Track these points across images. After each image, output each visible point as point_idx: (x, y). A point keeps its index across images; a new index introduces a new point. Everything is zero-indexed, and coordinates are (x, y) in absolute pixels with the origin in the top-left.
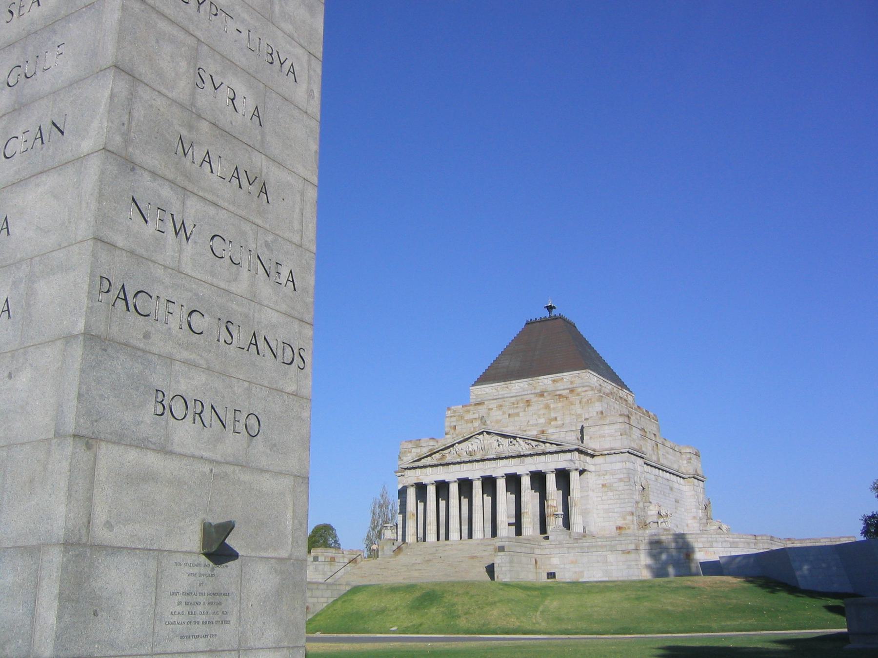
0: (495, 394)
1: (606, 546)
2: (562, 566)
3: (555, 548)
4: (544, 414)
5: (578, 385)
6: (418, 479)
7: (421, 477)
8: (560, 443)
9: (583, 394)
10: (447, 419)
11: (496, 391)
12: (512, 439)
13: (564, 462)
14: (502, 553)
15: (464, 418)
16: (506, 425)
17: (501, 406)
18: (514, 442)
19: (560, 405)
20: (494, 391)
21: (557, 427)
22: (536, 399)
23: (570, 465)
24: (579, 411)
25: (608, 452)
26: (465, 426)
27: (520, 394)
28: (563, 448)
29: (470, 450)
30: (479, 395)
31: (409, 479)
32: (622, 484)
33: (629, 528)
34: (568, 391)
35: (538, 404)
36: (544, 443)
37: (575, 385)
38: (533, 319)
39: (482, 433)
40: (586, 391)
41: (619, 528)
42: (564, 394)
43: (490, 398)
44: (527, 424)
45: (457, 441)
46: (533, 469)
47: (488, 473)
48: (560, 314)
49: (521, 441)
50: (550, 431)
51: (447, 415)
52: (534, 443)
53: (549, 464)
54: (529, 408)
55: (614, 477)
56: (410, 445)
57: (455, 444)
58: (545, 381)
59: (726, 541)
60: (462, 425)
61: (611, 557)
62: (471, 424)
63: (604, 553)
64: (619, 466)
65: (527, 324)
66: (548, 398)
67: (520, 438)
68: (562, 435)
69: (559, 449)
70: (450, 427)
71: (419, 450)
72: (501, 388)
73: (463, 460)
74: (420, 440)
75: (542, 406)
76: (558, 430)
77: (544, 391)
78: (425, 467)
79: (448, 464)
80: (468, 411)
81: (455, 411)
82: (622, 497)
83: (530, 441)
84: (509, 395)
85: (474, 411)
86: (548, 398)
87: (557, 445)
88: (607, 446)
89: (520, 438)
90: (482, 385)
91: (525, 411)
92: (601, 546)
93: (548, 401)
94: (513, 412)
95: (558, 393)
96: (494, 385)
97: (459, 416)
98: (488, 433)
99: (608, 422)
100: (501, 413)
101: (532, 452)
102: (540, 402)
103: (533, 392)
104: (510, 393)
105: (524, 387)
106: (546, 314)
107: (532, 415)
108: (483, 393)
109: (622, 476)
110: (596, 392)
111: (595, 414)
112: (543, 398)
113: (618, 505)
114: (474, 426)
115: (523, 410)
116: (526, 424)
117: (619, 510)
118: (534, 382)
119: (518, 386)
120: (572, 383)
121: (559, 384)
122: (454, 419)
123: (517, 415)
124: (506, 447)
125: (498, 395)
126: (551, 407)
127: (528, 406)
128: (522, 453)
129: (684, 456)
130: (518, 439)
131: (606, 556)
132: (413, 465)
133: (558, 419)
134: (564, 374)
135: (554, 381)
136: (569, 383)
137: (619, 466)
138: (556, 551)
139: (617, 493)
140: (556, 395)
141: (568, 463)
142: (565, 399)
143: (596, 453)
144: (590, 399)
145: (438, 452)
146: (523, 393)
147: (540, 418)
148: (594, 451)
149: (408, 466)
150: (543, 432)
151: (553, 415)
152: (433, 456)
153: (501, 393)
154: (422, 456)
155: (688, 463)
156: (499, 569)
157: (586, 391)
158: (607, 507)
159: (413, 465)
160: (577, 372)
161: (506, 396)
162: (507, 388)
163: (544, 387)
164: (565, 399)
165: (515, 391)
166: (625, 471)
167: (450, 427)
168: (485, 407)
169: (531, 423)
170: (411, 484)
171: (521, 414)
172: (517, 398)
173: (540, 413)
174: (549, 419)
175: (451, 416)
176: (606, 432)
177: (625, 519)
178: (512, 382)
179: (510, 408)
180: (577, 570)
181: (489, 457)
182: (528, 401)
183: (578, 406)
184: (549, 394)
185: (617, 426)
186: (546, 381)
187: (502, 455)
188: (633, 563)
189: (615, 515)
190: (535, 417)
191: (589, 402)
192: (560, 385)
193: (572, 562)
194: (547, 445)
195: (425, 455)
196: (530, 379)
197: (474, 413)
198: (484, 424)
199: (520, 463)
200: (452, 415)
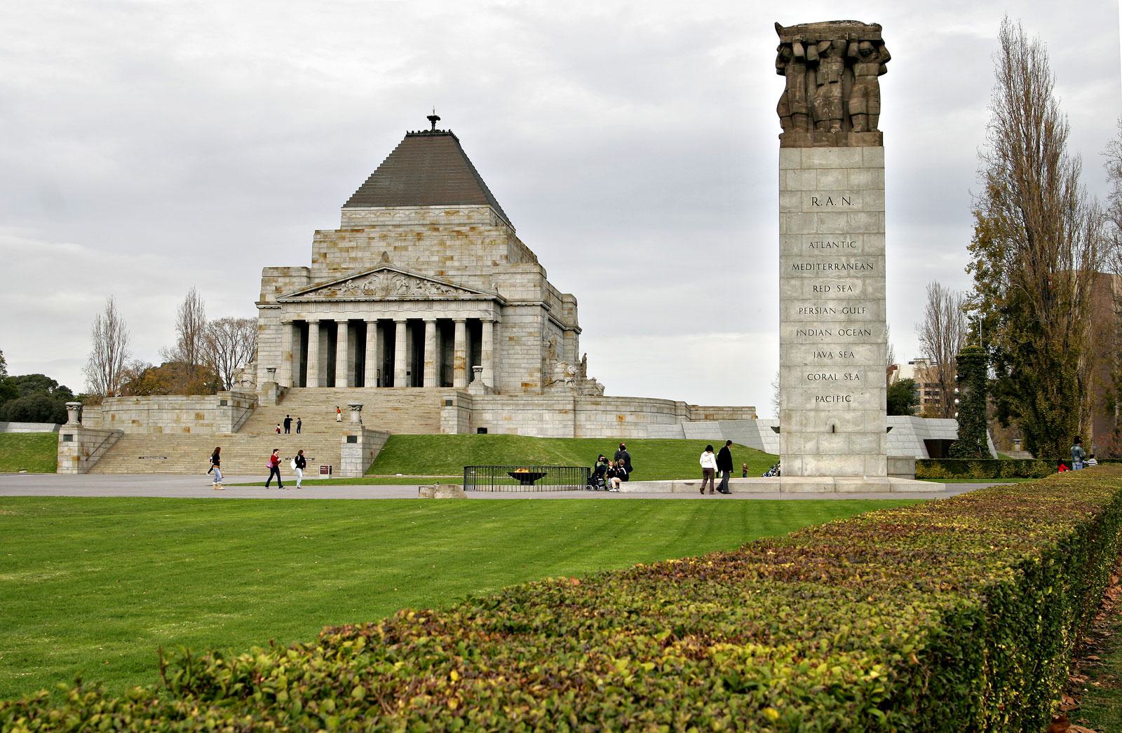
1: (542, 405)
2: (495, 422)
3: (488, 404)
4: (438, 251)
6: (299, 316)
7: (303, 314)
9: (486, 233)
10: (316, 244)
12: (418, 282)
14: (450, 407)
17: (385, 236)
19: (458, 243)
21: (458, 270)
22: (429, 233)
24: (480, 253)
25: (519, 303)
26: (338, 255)
27: (403, 223)
31: (287, 315)
32: (532, 338)
33: (536, 385)
34: (468, 228)
35: (431, 240)
37: (472, 221)
38: (416, 131)
39: (382, 271)
40: (489, 231)
41: (525, 385)
43: (367, 223)
46: (442, 316)
47: (387, 316)
49: (429, 284)
50: (451, 273)
52: (444, 288)
53: (459, 314)
55: (524, 330)
56: (276, 274)
58: (437, 212)
59: (654, 406)
60: (334, 253)
61: (547, 416)
62: (346, 254)
63: (540, 412)
64: (530, 319)
65: (409, 136)
68: (465, 279)
70: (319, 254)
71: (287, 280)
74: (289, 268)
75: (436, 242)
76: (459, 273)
78: (308, 302)
79: (337, 302)
80: (344, 238)
81: (325, 236)
82: (530, 352)
84: (390, 223)
86: (444, 234)
87: (472, 292)
88: (518, 297)
89: (428, 281)
92: (538, 405)
95: (457, 229)
96: (372, 208)
97: (331, 242)
98: (389, 271)
103: (421, 222)
106: (428, 126)
108: (358, 216)
109: (532, 330)
110: (502, 233)
111: (498, 258)
113: (525, 361)
117: (527, 366)
118: (423, 211)
119: (402, 214)
120: (469, 217)
121: (453, 218)
122: (324, 245)
123: (406, 248)
124: (415, 291)
127: (419, 239)
129: (565, 306)
131: (541, 415)
133: (455, 258)
134: (461, 206)
135: (447, 213)
137: (530, 319)
138: (490, 407)
139: (526, 347)
143: (508, 304)
145: (326, 287)
146: (409, 223)
147: (432, 255)
148: (505, 300)
150: (442, 273)
151: (449, 253)
153: (379, 219)
155: (569, 313)
156: (446, 423)
157: (489, 231)
158: (513, 361)
160: (477, 206)
161: (387, 223)
166: (535, 325)
167: (319, 254)
168: (364, 235)
169: (421, 259)
172: (407, 229)
176: (518, 281)
177: (531, 376)
180: (511, 426)
184: (445, 229)
185: (531, 277)
186: (437, 212)
188: (570, 423)
189: (522, 370)
191: (493, 243)
192: (455, 219)
193: (506, 419)
194: (461, 291)
196: (418, 207)
197: (350, 241)
198: (386, 261)
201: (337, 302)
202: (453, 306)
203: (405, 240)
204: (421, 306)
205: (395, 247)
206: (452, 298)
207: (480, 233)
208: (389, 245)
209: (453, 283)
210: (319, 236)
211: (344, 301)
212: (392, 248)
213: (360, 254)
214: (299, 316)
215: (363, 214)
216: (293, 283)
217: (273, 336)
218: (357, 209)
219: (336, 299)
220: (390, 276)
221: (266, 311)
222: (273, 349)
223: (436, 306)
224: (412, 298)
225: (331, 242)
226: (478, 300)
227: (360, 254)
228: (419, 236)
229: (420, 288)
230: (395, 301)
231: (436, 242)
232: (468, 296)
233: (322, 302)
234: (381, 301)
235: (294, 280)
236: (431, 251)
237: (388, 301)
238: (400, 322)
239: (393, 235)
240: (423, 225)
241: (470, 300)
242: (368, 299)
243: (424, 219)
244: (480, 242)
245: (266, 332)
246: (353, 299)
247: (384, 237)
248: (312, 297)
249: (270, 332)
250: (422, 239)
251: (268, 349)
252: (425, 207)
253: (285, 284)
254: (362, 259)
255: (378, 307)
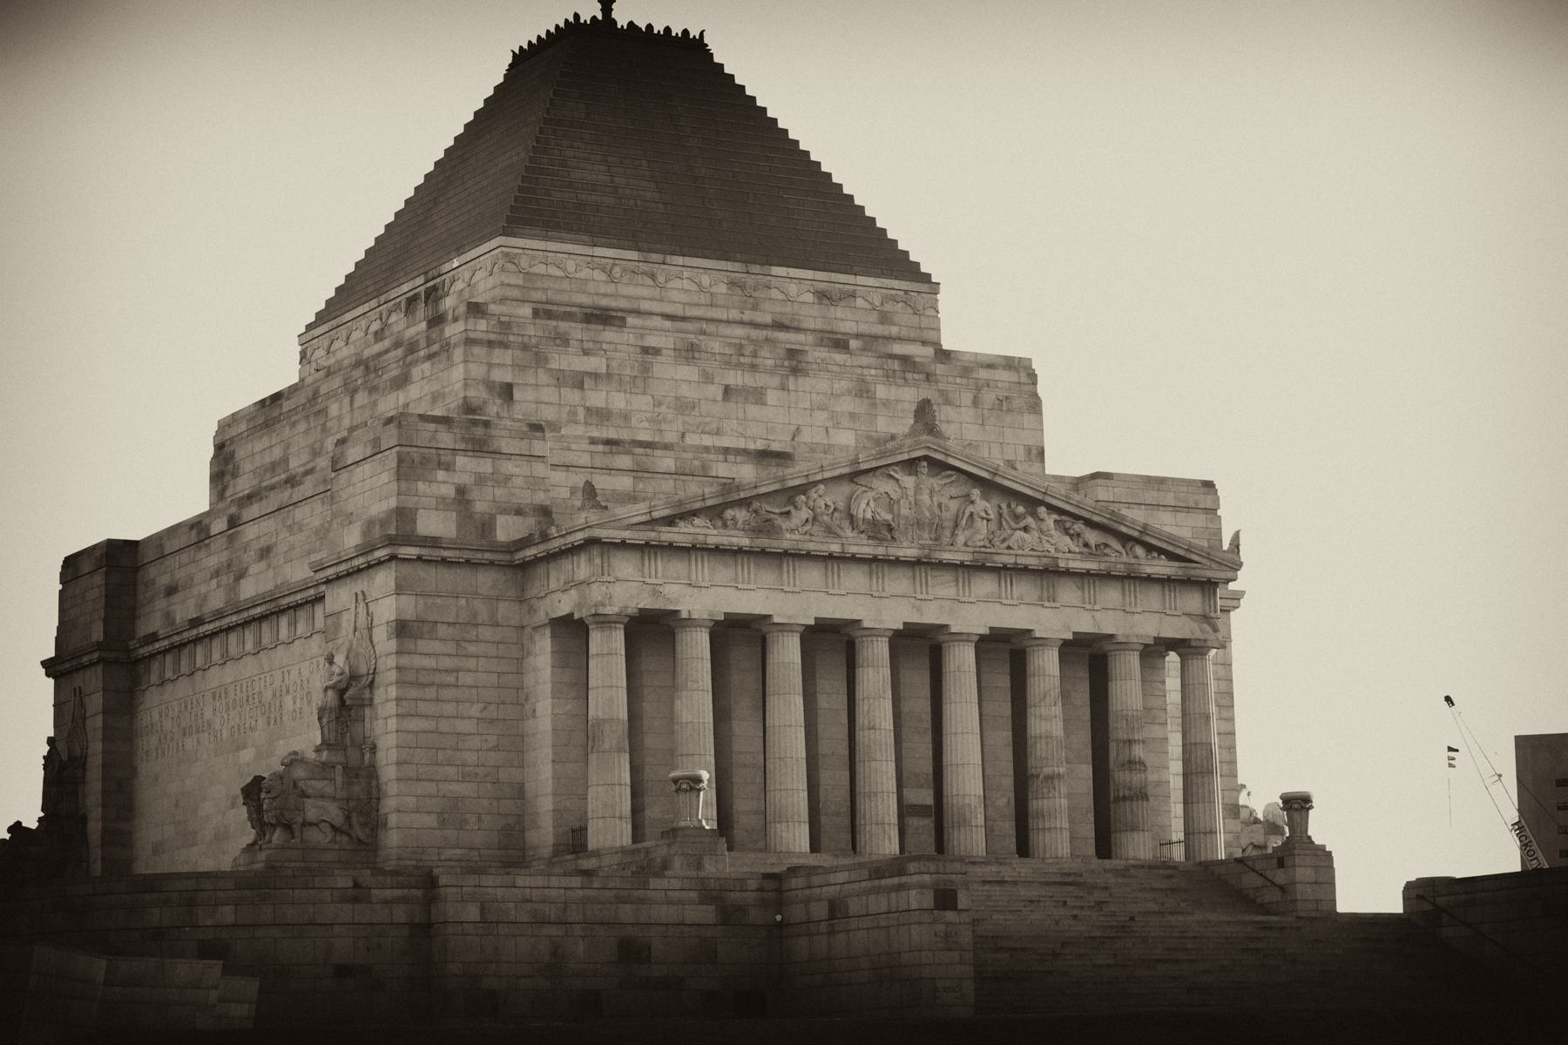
0: (602, 290)
4: (852, 416)
5: (904, 333)
6: (656, 593)
8: (1181, 553)
9: (983, 374)
10: (477, 350)
11: (603, 277)
12: (1021, 509)
13: (1187, 618)
15: (546, 360)
16: (714, 426)
18: (1030, 520)
20: (599, 275)
23: (1202, 631)
26: (549, 394)
28: (1192, 572)
29: (869, 516)
30: (537, 275)
36: (1125, 539)
37: (894, 330)
42: (917, 359)
44: (793, 439)
45: (827, 475)
46: (1085, 624)
48: (702, 33)
49: (1050, 520)
51: (472, 335)
52: (1093, 537)
54: (801, 380)
56: (446, 439)
57: (815, 484)
66: (865, 360)
67: (1052, 508)
69: (1180, 573)
70: (490, 385)
71: (485, 466)
72: (624, 270)
73: (853, 549)
77: (787, 322)
80: (563, 340)
81: (506, 326)
83: (1078, 527)
85: (586, 345)
89: (1052, 508)
90: (547, 239)
91: (783, 388)
93: (866, 372)
94: (740, 383)
95: (898, 349)
96: (598, 251)
98: (938, 466)
99: (1169, 499)
100: (696, 378)
101: (1091, 565)
102: (835, 368)
103: (748, 316)
104: (661, 300)
105: (713, 290)
107: (812, 409)
111: (1021, 452)
112: (844, 357)
114: (587, 405)
115: (776, 381)
116: (789, 438)
118: (750, 280)
120: (885, 318)
121: (839, 312)
122: (499, 356)
123: (758, 396)
125: (615, 296)
126: (878, 396)
127: (795, 371)
128: (1062, 564)
130: (1042, 510)
132: (653, 535)
134: (861, 280)
135: (823, 296)
136: (875, 315)
140: (892, 357)
141: (1195, 625)
142: (922, 376)
144: (1007, 398)
147: (837, 425)
149: (627, 534)
152: (729, 513)
154: (689, 507)
159: (653, 535)
161: (645, 306)
162: (653, 277)
163: (788, 309)
164: (922, 376)
165: (684, 298)
167: (490, 385)
168: (627, 337)
170: (630, 611)
171: (772, 396)
173: (837, 408)
174: (869, 438)
175: (490, 344)
178: (669, 259)
179: (728, 364)
181: (947, 556)
182: (792, 353)
183: (967, 414)
185: (1200, 520)
186: (793, 288)
187: (996, 558)
190: (821, 417)
191: (1003, 404)
194: (1139, 551)
195: (698, 505)
196: (737, 266)
197: (586, 353)
199: (1040, 598)
200: (492, 337)
201: (786, 555)
202: (1112, 595)
203: (754, 367)
204: (1024, 589)
205: (727, 390)
206: (1120, 569)
207: (966, 371)
208: (707, 378)
209: (1121, 520)
210: (482, 325)
211: (809, 556)
212: (715, 391)
213: (618, 401)
214: (656, 593)
215: (571, 265)
216: (508, 478)
217: (448, 663)
218: (552, 246)
219: (786, 545)
220: (936, 482)
221: (421, 571)
222: (449, 709)
223: (1068, 593)
224: (1009, 560)
225: (525, 347)
226: (1187, 583)
227: (618, 401)
228: (795, 363)
229: (1026, 529)
230: (962, 565)
231: (843, 383)
232: (1161, 567)
233: (737, 553)
234: (916, 564)
235: (509, 467)
236: (833, 416)
237: (942, 566)
238: (961, 637)
239: (716, 346)
240: (754, 325)
241: (1166, 582)
242: (880, 551)
243: (755, 308)
244: (967, 398)
245: (423, 645)
246: (835, 548)
247: (689, 353)
248: (699, 530)
249: (436, 646)
250: (805, 373)
251: (430, 708)
252: (756, 268)
253: (481, 480)
254: (626, 417)
255: (899, 583)
